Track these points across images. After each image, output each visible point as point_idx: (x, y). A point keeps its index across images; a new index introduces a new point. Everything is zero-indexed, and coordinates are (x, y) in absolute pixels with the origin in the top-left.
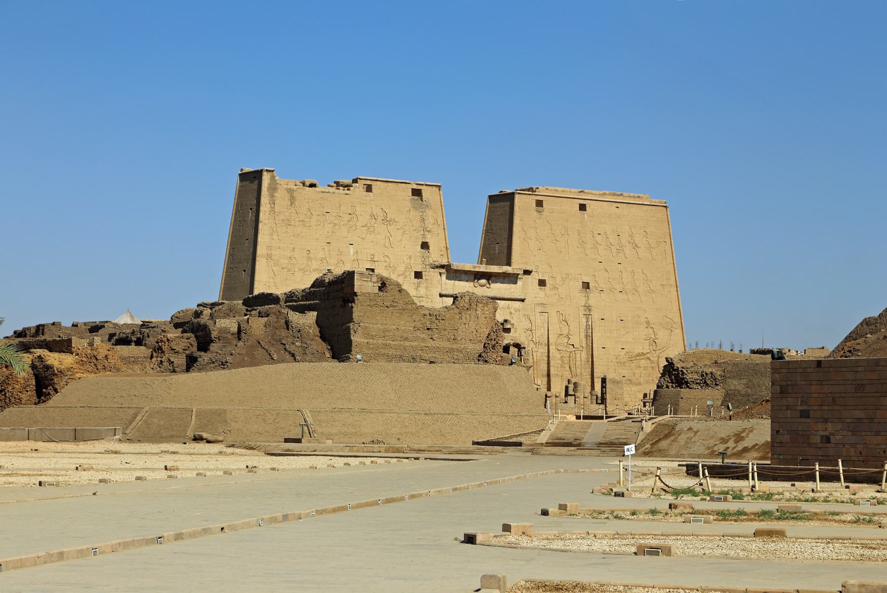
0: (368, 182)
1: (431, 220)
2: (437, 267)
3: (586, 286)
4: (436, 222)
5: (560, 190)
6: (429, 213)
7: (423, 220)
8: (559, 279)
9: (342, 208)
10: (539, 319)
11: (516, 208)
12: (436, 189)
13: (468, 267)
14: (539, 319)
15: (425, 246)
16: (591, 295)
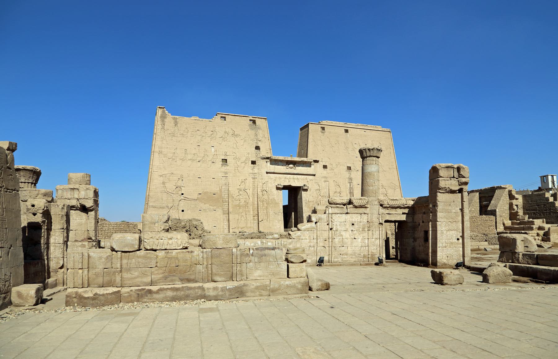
0: (224, 116)
2: (264, 158)
3: (349, 168)
4: (264, 136)
5: (334, 123)
6: (260, 132)
7: (256, 135)
8: (334, 165)
9: (207, 128)
10: (323, 184)
11: (310, 130)
12: (265, 120)
13: (281, 158)
14: (323, 184)
15: (257, 148)
16: (352, 173)
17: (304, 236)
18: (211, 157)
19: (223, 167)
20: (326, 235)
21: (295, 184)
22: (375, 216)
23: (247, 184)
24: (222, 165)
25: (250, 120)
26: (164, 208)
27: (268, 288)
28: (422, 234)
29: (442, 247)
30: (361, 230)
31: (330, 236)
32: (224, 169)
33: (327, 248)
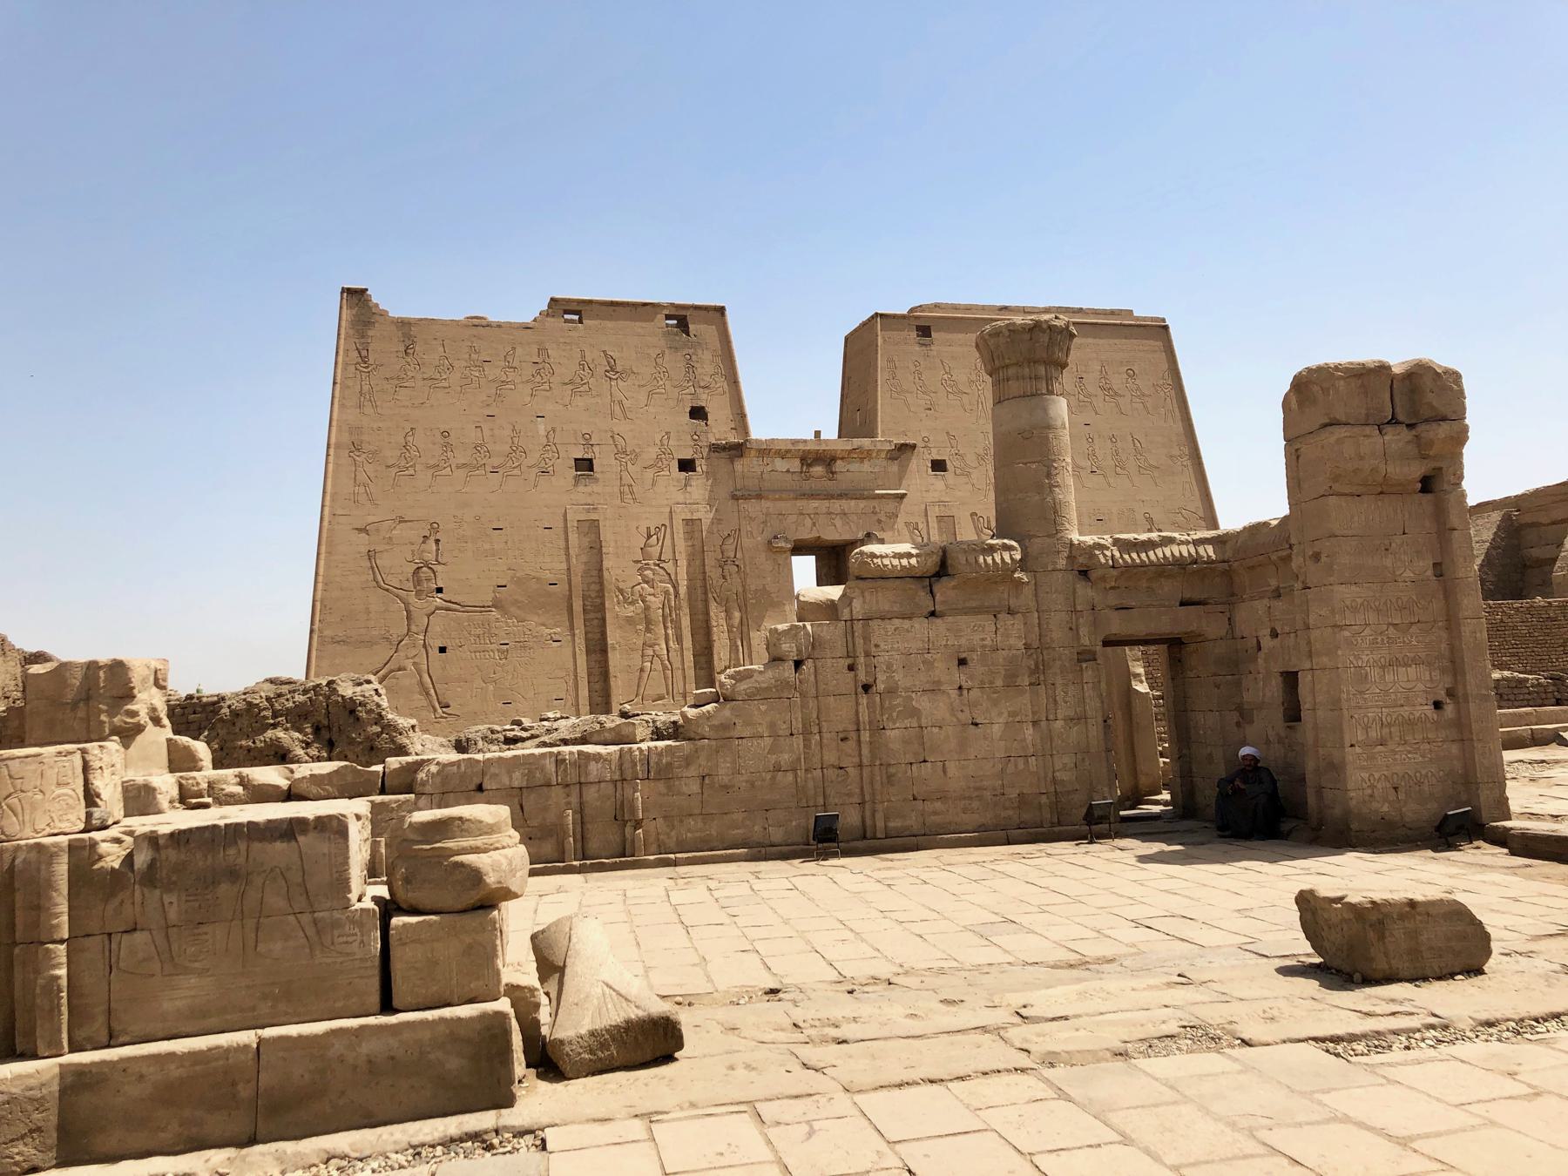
1: (709, 369)
15: (698, 413)
17: (747, 724)
18: (533, 458)
19: (581, 488)
20: (840, 713)
21: (834, 533)
22: (1057, 622)
23: (668, 542)
24: (577, 479)
25: (668, 317)
26: (371, 643)
27: (245, 1092)
28: (1273, 690)
29: (1368, 744)
30: (999, 683)
31: (864, 716)
32: (584, 492)
33: (852, 771)
